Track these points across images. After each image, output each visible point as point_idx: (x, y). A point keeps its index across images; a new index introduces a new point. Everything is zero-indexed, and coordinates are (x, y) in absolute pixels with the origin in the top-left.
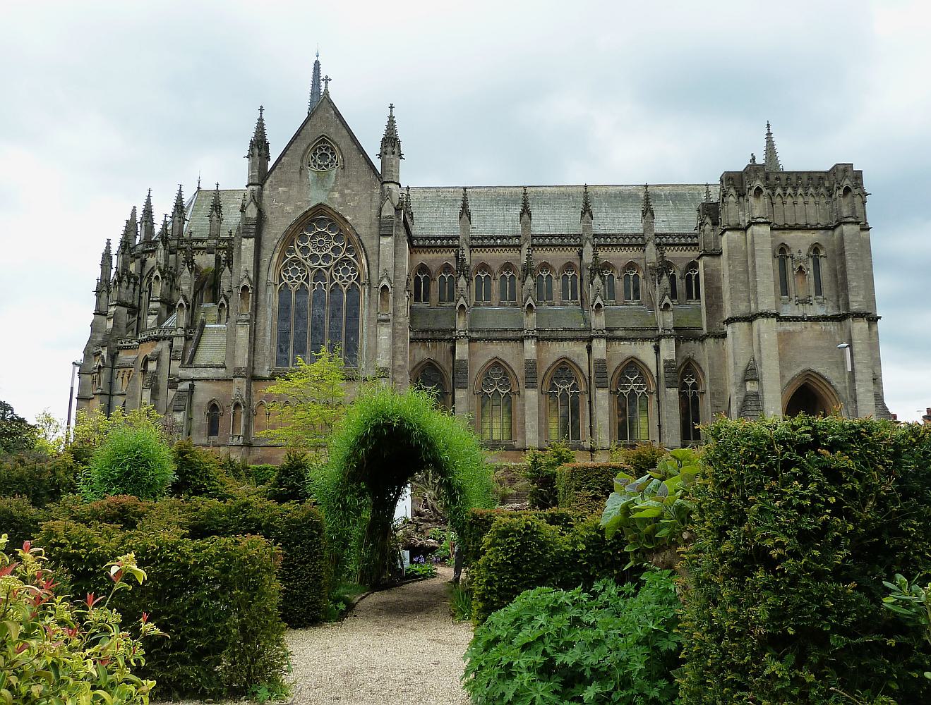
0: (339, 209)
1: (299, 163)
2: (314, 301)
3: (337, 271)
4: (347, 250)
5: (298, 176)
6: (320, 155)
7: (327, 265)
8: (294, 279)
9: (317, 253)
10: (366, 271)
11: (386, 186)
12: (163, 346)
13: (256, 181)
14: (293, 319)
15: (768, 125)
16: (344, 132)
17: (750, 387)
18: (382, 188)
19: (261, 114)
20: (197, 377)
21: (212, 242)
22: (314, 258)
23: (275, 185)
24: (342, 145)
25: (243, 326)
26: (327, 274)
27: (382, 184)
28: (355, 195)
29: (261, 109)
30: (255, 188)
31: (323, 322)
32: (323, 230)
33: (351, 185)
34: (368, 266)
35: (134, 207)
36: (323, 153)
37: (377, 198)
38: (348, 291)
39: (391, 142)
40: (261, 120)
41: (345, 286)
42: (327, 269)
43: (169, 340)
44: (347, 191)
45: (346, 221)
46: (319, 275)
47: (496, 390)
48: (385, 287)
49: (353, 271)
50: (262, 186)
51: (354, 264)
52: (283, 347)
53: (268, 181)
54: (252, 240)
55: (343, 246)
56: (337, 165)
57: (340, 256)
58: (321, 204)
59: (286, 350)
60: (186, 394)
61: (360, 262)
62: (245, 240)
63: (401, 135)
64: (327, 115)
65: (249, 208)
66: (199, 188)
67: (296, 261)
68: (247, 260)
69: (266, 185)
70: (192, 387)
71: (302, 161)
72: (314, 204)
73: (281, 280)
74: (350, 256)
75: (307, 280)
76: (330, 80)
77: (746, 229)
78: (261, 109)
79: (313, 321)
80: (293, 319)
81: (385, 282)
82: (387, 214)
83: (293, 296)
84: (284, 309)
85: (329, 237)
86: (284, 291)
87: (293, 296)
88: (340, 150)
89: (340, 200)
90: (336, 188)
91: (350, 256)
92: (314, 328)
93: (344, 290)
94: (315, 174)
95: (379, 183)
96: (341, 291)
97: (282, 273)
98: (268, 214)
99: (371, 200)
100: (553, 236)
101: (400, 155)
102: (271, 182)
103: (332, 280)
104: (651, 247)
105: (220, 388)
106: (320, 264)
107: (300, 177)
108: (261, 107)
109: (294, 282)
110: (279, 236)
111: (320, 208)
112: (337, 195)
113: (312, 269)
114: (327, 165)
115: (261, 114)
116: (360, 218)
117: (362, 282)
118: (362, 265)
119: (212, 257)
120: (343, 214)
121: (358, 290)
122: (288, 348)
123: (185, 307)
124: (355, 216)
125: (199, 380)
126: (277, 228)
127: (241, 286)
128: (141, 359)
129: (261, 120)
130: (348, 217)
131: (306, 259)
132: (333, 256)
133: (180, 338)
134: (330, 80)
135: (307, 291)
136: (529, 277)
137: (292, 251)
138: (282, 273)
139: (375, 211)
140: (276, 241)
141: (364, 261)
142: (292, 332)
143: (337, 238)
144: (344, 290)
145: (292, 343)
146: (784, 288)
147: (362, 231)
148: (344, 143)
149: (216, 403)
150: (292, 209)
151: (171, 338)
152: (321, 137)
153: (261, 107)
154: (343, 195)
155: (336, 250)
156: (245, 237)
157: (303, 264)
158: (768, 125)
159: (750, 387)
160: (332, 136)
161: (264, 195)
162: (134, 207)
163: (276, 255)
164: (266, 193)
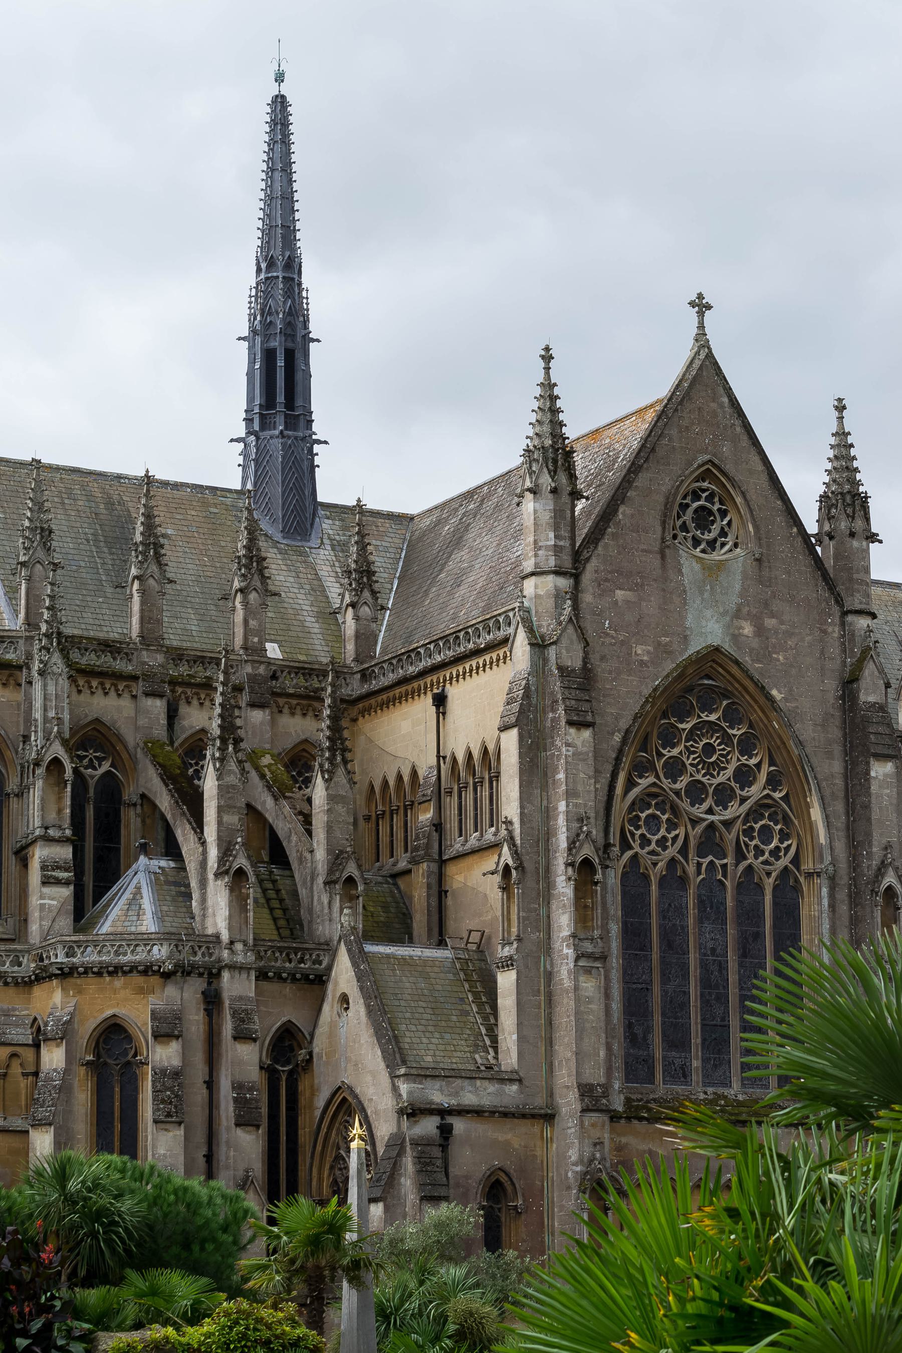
0: (755, 667)
1: (659, 529)
2: (701, 904)
3: (748, 833)
4: (773, 782)
5: (657, 562)
6: (696, 511)
8: (653, 845)
9: (699, 777)
10: (823, 838)
11: (850, 618)
14: (655, 955)
16: (756, 459)
18: (843, 624)
19: (547, 369)
20: (453, 1102)
21: (154, 660)
22: (696, 791)
23: (607, 580)
24: (752, 495)
25: (588, 971)
26: (730, 837)
27: (845, 614)
28: (789, 634)
31: (722, 967)
32: (713, 717)
33: (776, 605)
34: (828, 826)
36: (702, 508)
37: (834, 650)
38: (776, 888)
40: (548, 386)
41: (769, 874)
42: (728, 824)
43: (201, 975)
44: (770, 623)
45: (771, 699)
48: (890, 888)
49: (784, 836)
51: (786, 820)
52: (638, 1031)
53: (591, 567)
54: (587, 734)
55: (758, 765)
56: (736, 545)
57: (756, 791)
58: (717, 649)
59: (645, 1038)
60: (436, 1152)
62: (572, 731)
63: (868, 482)
64: (714, 405)
65: (564, 642)
67: (654, 796)
68: (580, 788)
69: (587, 577)
70: (446, 1131)
71: (664, 523)
72: (696, 646)
74: (777, 795)
75: (684, 851)
76: (709, 307)
78: (547, 357)
79: (704, 965)
80: (655, 955)
81: (890, 879)
82: (872, 699)
83: (654, 888)
85: (727, 739)
87: (654, 888)
88: (751, 511)
89: (755, 643)
90: (745, 610)
91: (777, 795)
92: (706, 983)
94: (697, 567)
95: (836, 610)
96: (760, 888)
97: (628, 827)
98: (594, 658)
99: (822, 653)
101: (873, 538)
103: (740, 856)
105: (509, 1136)
106: (710, 811)
107: (664, 566)
108: (547, 349)
109: (652, 853)
110: (624, 724)
112: (748, 629)
113: (695, 822)
115: (547, 369)
117: (808, 865)
118: (811, 827)
119: (158, 706)
120: (765, 682)
121: (797, 889)
122: (648, 1030)
123: (252, 879)
124: (791, 690)
125: (461, 1112)
128: (87, 1028)
129: (548, 386)
130: (774, 692)
131: (677, 793)
132: (738, 791)
133: (244, 975)
134: (709, 307)
135: (683, 880)
137: (641, 768)
138: (628, 827)
139: (831, 686)
140: (618, 737)
141: (816, 814)
142: (656, 989)
145: (657, 1019)
147: (807, 731)
148: (757, 485)
149: (503, 1178)
150: (648, 652)
151: (212, 974)
152: (703, 465)
153: (547, 349)
154: (760, 631)
155: (744, 776)
156: (570, 723)
157: (675, 810)
160: (729, 468)
161: (583, 606)
164: (587, 598)
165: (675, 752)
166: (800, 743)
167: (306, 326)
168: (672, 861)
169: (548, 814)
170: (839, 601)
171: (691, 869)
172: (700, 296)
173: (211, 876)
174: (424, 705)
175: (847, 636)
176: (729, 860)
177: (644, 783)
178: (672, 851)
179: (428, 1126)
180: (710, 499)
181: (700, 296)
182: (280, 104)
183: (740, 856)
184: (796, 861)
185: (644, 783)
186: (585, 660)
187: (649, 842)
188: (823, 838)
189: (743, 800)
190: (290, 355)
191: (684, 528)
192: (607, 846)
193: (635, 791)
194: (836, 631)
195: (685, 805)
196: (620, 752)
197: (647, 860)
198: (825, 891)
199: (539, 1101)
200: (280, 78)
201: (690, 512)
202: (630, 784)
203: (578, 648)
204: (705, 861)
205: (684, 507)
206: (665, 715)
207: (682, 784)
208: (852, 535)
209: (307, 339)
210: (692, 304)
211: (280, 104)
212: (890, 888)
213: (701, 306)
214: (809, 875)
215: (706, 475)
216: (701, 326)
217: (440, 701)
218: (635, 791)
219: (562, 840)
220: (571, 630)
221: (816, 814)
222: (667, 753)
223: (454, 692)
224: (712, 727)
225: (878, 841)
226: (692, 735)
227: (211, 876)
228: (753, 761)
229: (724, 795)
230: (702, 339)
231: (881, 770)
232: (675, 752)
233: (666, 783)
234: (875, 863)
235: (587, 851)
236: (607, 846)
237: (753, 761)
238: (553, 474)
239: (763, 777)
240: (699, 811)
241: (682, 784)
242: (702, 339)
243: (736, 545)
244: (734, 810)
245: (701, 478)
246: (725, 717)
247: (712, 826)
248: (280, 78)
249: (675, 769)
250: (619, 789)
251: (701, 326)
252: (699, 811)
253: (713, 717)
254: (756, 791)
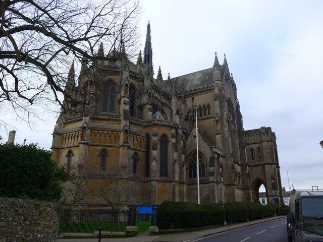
12: (173, 131)
17: (273, 181)
40: (216, 57)
78: (216, 53)
128: (160, 134)
129: (216, 57)
151: (177, 129)
159: (273, 181)
173: (174, 115)
182: (149, 26)
190: (149, 55)
199: (223, 155)
209: (151, 53)
211: (149, 26)
217: (193, 99)
219: (225, 117)
223: (195, 98)
227: (174, 115)
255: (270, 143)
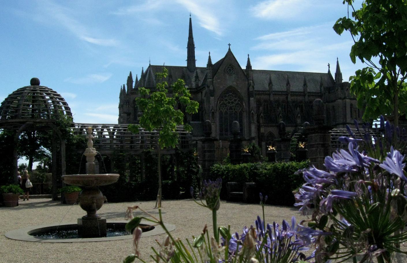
0: (236, 87)
4: (239, 101)
7: (233, 105)
13: (211, 77)
15: (337, 58)
16: (237, 64)
18: (248, 82)
19: (210, 54)
22: (229, 103)
25: (213, 124)
26: (233, 108)
29: (209, 53)
30: (210, 80)
32: (231, 94)
34: (246, 106)
35: (131, 72)
36: (229, 69)
39: (249, 66)
40: (210, 57)
45: (238, 92)
46: (231, 108)
47: (270, 142)
48: (252, 113)
50: (213, 79)
53: (214, 78)
54: (213, 97)
55: (237, 99)
57: (236, 102)
61: (242, 104)
66: (150, 64)
69: (214, 79)
70: (197, 143)
72: (228, 85)
73: (220, 110)
75: (227, 110)
76: (230, 45)
77: (343, 99)
78: (209, 53)
84: (221, 118)
85: (233, 96)
86: (221, 113)
91: (239, 102)
93: (238, 113)
100: (279, 92)
102: (215, 78)
103: (235, 110)
104: (306, 97)
106: (231, 105)
108: (210, 52)
110: (219, 96)
111: (231, 87)
112: (235, 83)
113: (229, 106)
114: (231, 73)
116: (243, 92)
117: (243, 110)
121: (242, 113)
126: (218, 93)
127: (212, 112)
129: (210, 57)
130: (239, 91)
134: (230, 45)
136: (280, 107)
140: (218, 97)
143: (235, 97)
144: (238, 113)
146: (351, 117)
153: (210, 52)
155: (235, 100)
157: (226, 105)
158: (337, 58)
162: (131, 72)
163: (219, 101)
164: (214, 81)
165: (226, 98)
166: (242, 96)
167: (194, 45)
168: (226, 111)
169: (209, 107)
170: (247, 78)
171: (228, 112)
172: (229, 44)
174: (200, 93)
175: (248, 83)
176: (233, 110)
177: (222, 102)
178: (226, 110)
179: (195, 142)
180: (231, 68)
181: (229, 44)
182: (190, 19)
183: (235, 110)
184: (242, 110)
185: (222, 102)
186: (214, 88)
187: (223, 109)
188: (245, 107)
189: (235, 103)
191: (227, 72)
192: (217, 110)
193: (221, 103)
194: (247, 82)
195: (227, 104)
196: (218, 99)
197: (223, 111)
198: (245, 113)
200: (190, 15)
201: (228, 70)
202: (220, 103)
203: (213, 87)
204: (230, 111)
205: (227, 69)
206: (225, 94)
207: (227, 102)
208: (249, 71)
210: (228, 45)
211: (190, 19)
212: (252, 113)
213: (229, 45)
214: (243, 111)
215: (229, 65)
216: (229, 47)
218: (221, 103)
220: (211, 86)
221: (244, 104)
222: (225, 98)
224: (231, 95)
225: (251, 107)
226: (228, 96)
228: (236, 99)
229: (232, 103)
230: (229, 49)
231: (252, 99)
232: (226, 98)
233: (225, 102)
234: (251, 109)
235: (213, 111)
236: (217, 110)
237: (236, 99)
238: (209, 67)
239: (237, 100)
240: (229, 105)
241: (227, 102)
242: (229, 49)
243: (234, 73)
244: (234, 105)
245: (229, 65)
246: (233, 94)
247: (231, 107)
248: (190, 15)
249: (226, 100)
250: (218, 103)
251: (229, 47)
252: (229, 105)
253: (231, 94)
254: (236, 102)
255: (344, 100)
